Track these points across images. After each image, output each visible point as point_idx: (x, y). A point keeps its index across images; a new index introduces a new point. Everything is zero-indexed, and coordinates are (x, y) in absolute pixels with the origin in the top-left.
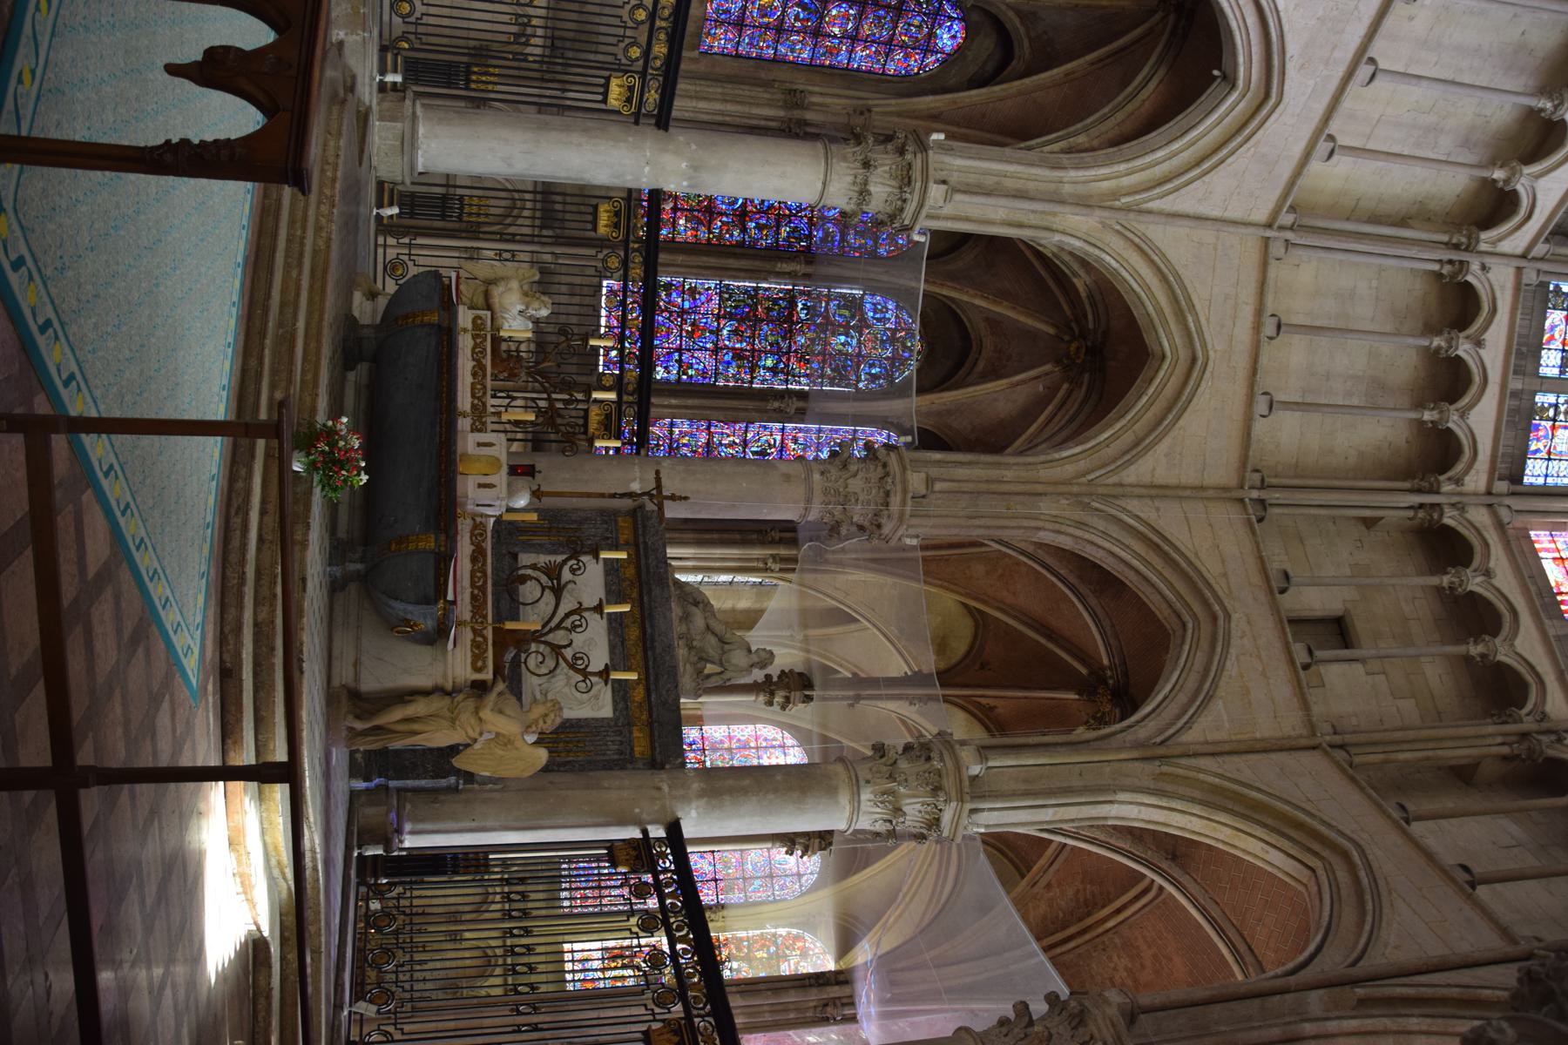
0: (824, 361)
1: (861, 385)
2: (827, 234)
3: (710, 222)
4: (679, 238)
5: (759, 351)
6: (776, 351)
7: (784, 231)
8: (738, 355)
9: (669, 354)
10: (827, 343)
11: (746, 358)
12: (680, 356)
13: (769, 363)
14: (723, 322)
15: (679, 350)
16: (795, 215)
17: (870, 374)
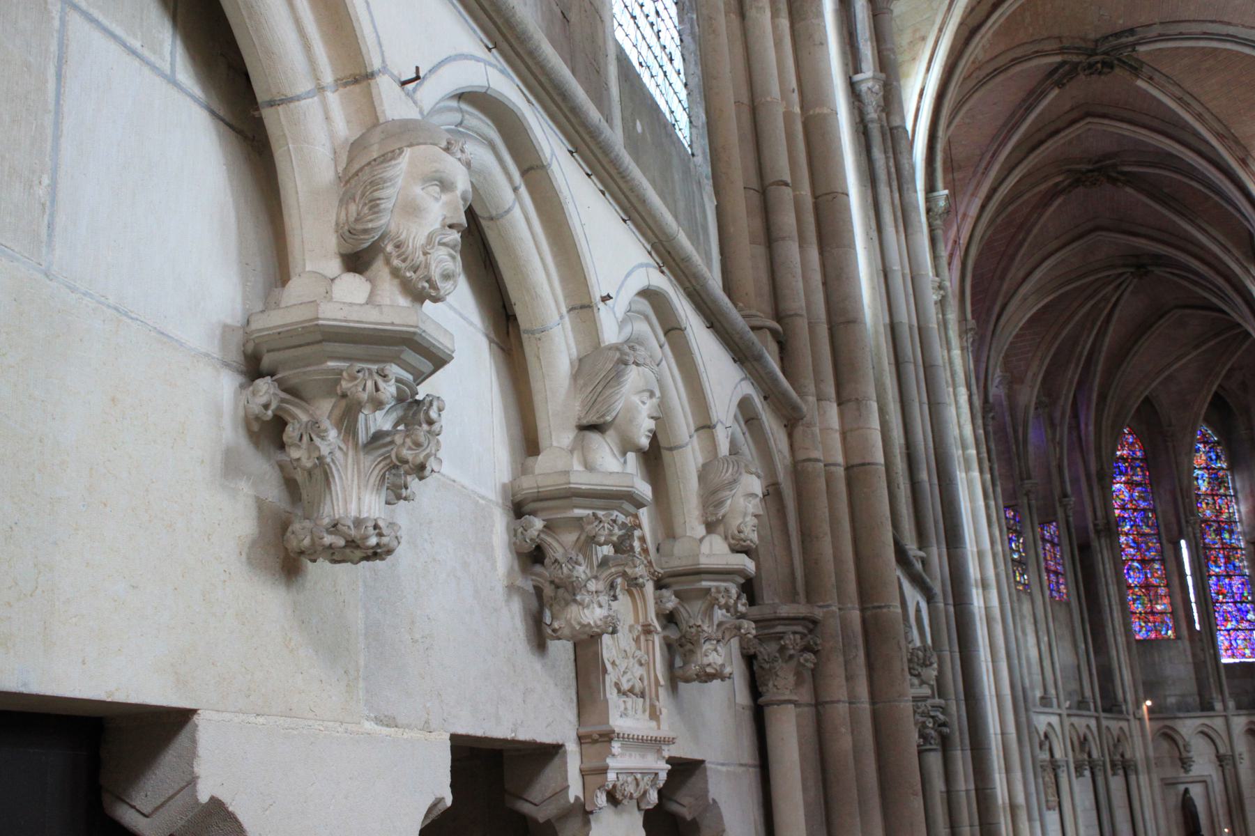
0: (1217, 495)
1: (1225, 466)
2: (1140, 497)
3: (1153, 586)
4: (1169, 609)
5: (1223, 544)
6: (1219, 532)
7: (1147, 530)
8: (1227, 558)
9: (1239, 610)
10: (1206, 495)
11: (1228, 553)
12: (1238, 602)
13: (1226, 536)
14: (1212, 573)
15: (1235, 603)
16: (1135, 521)
17: (1216, 460)
